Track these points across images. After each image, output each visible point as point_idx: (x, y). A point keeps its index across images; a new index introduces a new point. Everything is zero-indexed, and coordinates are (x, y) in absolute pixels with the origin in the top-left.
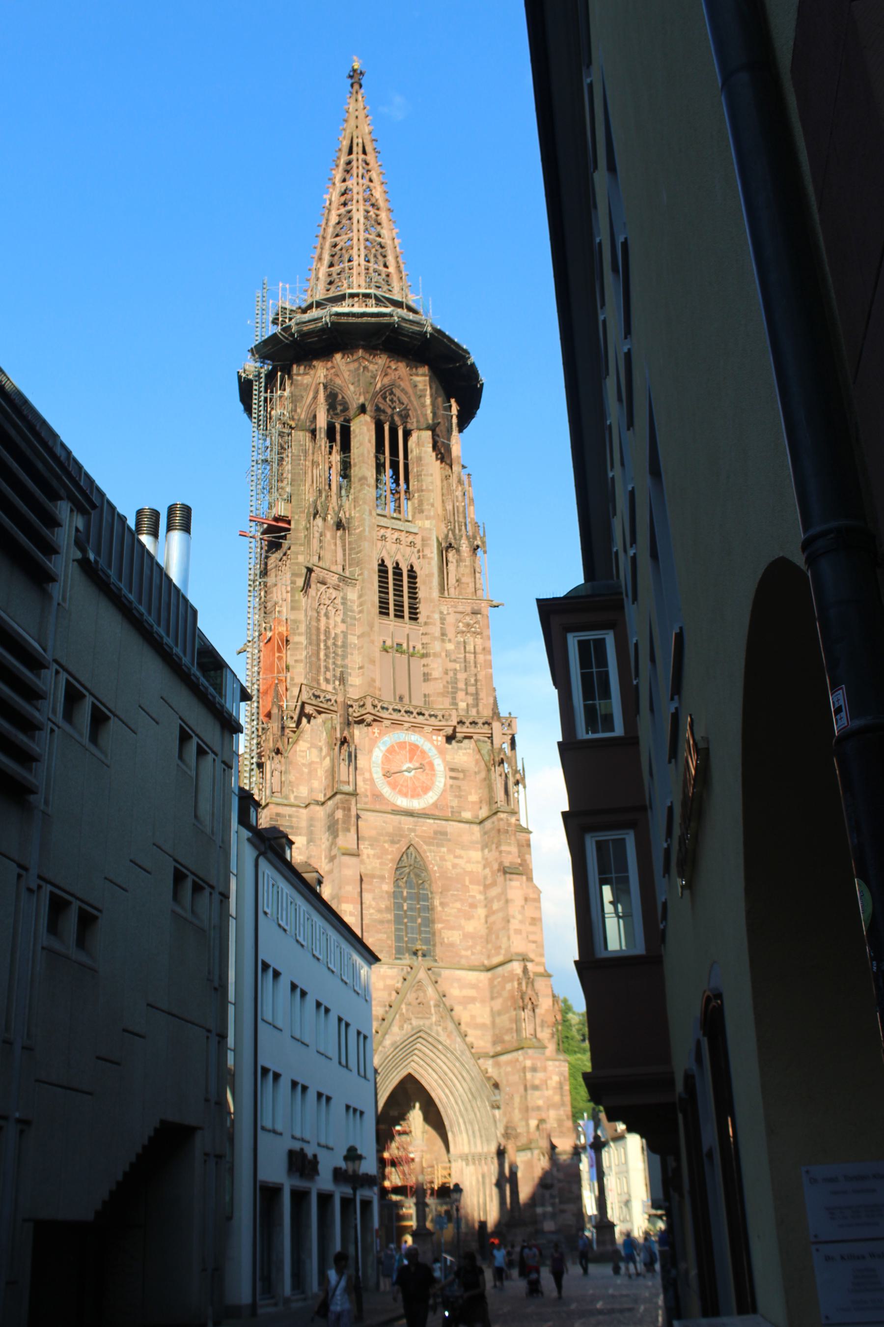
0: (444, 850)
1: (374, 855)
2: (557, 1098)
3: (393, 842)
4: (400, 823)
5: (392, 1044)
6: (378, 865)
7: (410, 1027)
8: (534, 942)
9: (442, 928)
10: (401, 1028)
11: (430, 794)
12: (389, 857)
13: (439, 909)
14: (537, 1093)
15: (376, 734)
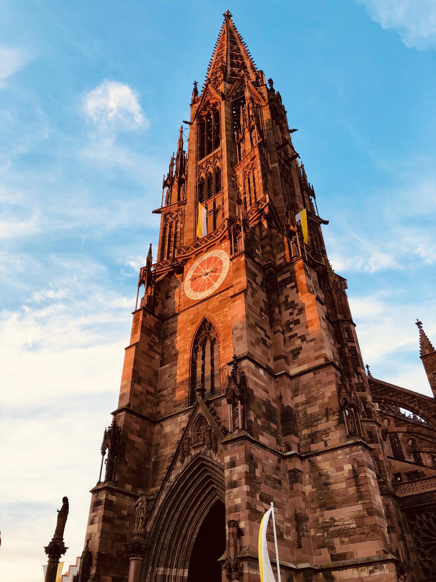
0: (227, 308)
1: (181, 339)
2: (352, 490)
3: (192, 325)
4: (198, 309)
5: (176, 478)
6: (183, 345)
7: (189, 457)
8: (311, 341)
9: (224, 366)
10: (182, 461)
11: (219, 280)
12: (190, 335)
13: (222, 352)
14: (235, 490)
15: (189, 267)
